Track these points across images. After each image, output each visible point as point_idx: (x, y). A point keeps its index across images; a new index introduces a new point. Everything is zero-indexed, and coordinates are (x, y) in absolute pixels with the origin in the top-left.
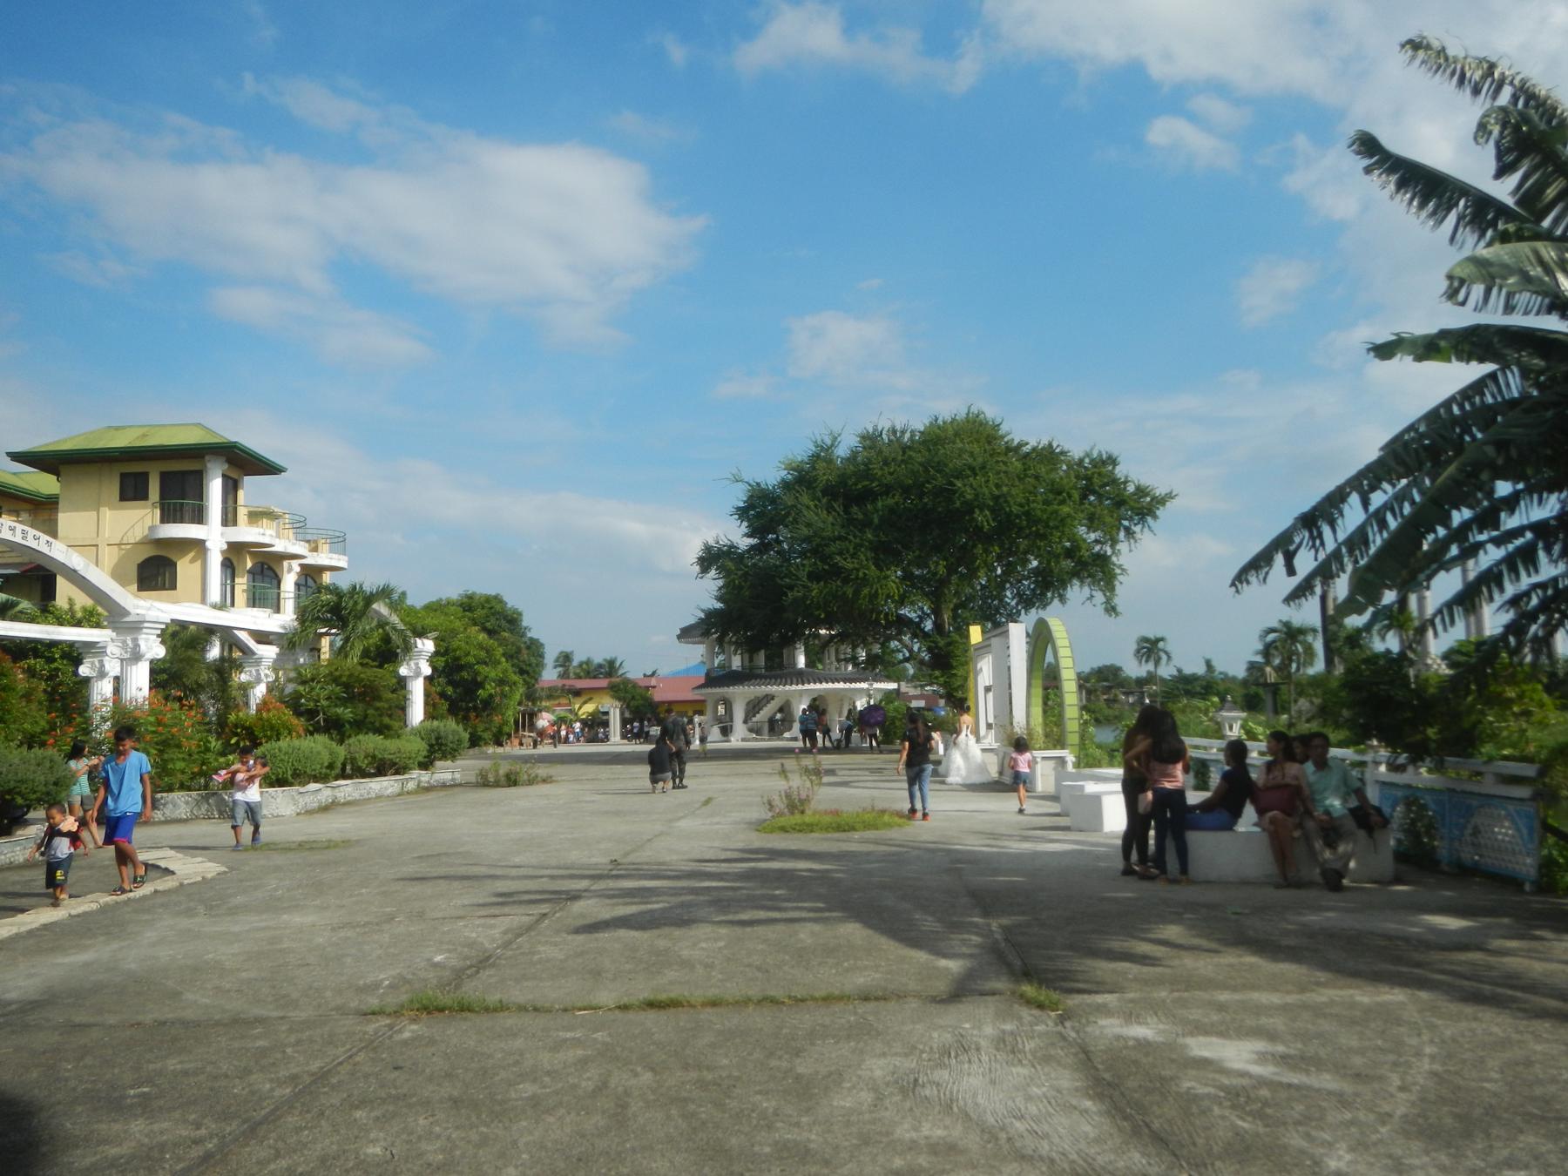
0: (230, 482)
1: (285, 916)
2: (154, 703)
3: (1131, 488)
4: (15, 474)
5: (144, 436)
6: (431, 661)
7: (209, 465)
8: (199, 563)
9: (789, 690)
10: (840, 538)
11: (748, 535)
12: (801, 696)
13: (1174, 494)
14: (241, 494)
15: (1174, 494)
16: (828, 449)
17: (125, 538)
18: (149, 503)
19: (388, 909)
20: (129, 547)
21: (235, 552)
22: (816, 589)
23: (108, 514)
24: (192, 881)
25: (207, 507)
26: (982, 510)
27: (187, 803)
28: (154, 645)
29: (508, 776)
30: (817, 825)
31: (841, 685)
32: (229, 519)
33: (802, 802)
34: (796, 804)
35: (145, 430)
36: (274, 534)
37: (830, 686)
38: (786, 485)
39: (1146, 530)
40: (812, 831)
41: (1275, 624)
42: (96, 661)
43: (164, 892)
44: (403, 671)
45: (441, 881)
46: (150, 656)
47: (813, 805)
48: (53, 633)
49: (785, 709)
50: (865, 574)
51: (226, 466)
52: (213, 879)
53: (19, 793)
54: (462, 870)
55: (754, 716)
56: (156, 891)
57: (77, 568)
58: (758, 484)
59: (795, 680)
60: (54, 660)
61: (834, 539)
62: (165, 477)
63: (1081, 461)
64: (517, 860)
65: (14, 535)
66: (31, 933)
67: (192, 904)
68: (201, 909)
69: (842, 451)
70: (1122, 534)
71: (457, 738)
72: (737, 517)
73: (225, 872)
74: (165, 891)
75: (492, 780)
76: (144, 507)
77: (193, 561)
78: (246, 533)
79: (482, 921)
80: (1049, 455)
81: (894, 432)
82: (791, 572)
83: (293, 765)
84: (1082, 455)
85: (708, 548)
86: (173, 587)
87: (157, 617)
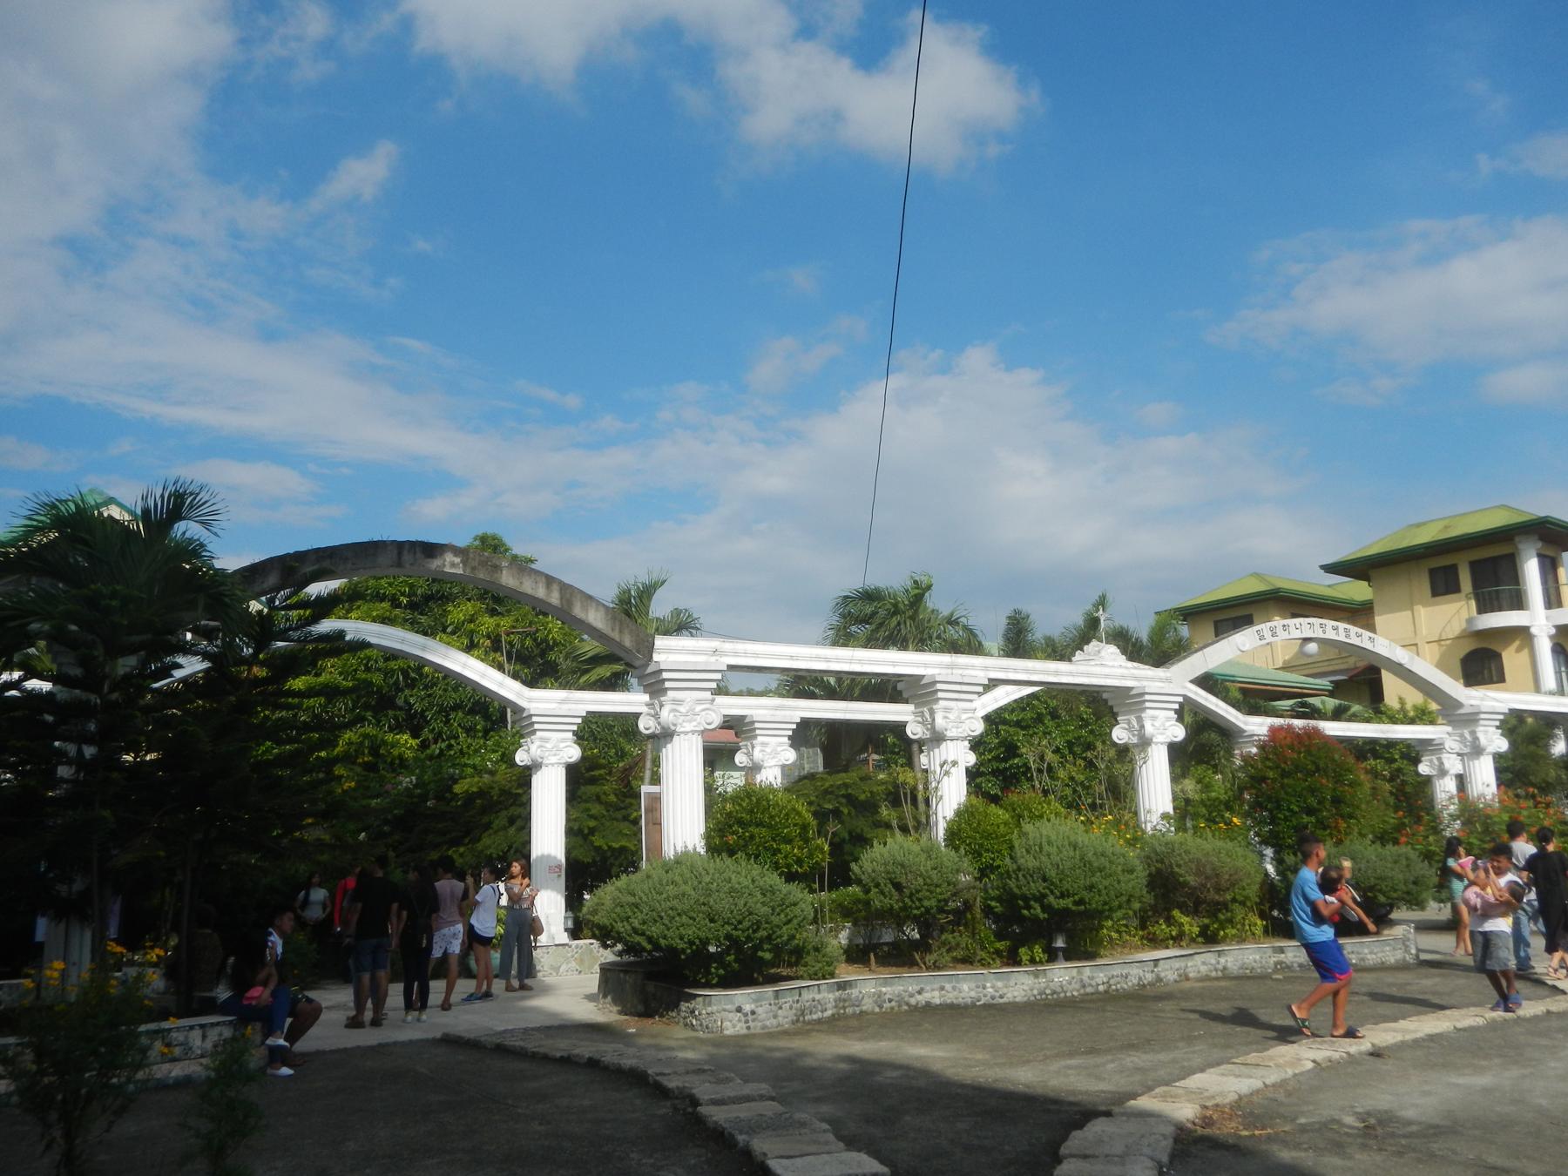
0: (1548, 562)
2: (1504, 801)
4: (1329, 586)
5: (1446, 527)
7: (1521, 546)
14: (1562, 572)
17: (1443, 634)
18: (1462, 595)
20: (1448, 642)
23: (1423, 612)
25: (1525, 591)
28: (1495, 737)
35: (1445, 522)
42: (1434, 758)
46: (1492, 749)
48: (1388, 732)
51: (1540, 545)
53: (1380, 891)
56: (1549, 1012)
57: (1403, 662)
60: (1393, 761)
62: (1475, 567)
65: (1337, 634)
66: (1417, 1043)
76: (1460, 600)
77: (1518, 650)
86: (1502, 679)
87: (1493, 706)
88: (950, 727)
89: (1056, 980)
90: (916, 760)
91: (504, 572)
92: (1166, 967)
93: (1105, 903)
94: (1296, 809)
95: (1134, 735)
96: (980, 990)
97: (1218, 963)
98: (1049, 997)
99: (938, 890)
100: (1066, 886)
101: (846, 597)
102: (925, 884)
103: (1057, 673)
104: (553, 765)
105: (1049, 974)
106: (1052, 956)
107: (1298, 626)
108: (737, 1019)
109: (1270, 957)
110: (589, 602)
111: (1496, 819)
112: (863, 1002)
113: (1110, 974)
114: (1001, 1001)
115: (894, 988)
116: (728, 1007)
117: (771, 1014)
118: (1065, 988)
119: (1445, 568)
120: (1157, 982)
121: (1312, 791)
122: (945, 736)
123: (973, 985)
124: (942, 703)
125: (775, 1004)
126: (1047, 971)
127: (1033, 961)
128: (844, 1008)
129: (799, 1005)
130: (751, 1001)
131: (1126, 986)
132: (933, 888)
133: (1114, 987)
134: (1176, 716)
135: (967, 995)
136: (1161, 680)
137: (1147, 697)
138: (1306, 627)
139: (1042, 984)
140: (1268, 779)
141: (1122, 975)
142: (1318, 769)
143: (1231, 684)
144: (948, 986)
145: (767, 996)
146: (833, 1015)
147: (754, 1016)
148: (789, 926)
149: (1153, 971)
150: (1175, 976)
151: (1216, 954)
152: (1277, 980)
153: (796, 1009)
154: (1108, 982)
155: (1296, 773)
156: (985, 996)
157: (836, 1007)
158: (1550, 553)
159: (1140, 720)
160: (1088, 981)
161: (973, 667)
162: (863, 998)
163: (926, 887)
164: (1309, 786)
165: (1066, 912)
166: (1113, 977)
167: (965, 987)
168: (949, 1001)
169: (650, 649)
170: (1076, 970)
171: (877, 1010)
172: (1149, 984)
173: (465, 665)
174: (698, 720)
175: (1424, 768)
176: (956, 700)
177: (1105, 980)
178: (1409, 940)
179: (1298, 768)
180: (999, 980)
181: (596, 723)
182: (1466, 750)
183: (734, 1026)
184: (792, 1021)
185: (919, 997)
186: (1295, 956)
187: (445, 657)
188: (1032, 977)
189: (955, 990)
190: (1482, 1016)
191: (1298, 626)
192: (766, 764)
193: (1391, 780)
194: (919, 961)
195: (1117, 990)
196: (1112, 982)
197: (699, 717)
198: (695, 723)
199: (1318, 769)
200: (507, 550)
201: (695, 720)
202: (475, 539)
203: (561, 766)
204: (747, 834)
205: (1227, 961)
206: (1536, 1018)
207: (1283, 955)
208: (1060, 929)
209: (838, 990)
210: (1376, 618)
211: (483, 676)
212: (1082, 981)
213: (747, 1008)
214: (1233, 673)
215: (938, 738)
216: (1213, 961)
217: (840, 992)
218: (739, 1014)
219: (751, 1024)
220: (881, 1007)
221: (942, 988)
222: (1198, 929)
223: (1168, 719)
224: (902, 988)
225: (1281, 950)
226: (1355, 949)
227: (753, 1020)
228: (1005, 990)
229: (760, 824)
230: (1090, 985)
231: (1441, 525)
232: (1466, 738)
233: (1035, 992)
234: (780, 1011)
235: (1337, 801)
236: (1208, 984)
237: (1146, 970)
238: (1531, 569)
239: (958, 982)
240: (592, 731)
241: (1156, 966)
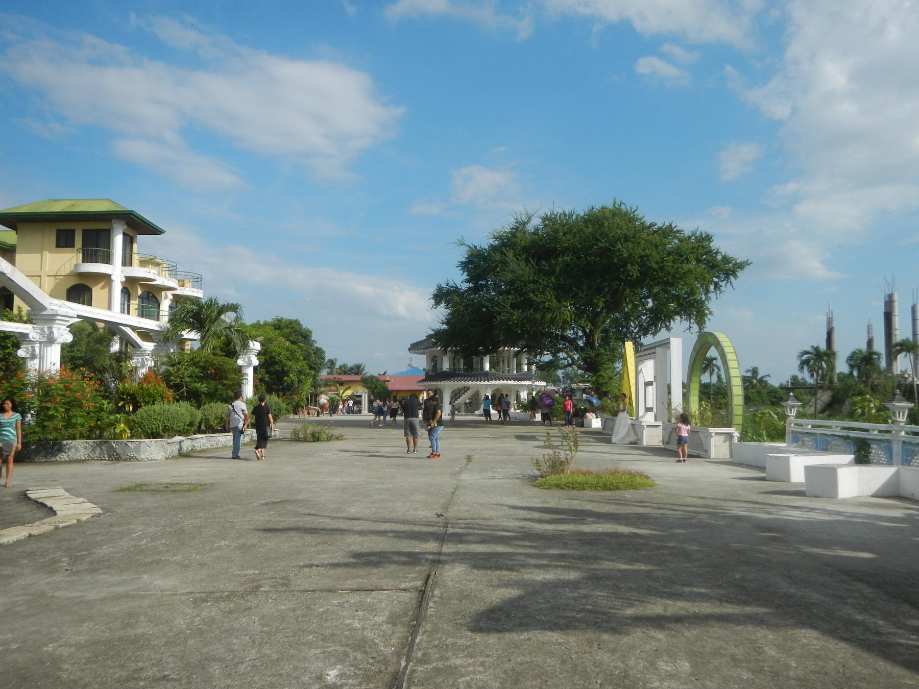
0: (128, 239)
1: (145, 577)
3: (719, 257)
5: (73, 205)
6: (259, 354)
7: (114, 226)
9: (480, 385)
10: (535, 282)
11: (468, 281)
12: (486, 388)
13: (749, 262)
14: (135, 246)
15: (749, 262)
16: (524, 224)
17: (59, 272)
18: (75, 249)
19: (251, 572)
20: (61, 277)
21: (130, 284)
22: (516, 314)
23: (48, 256)
24: (67, 524)
26: (632, 265)
27: (85, 448)
28: (64, 333)
29: (313, 435)
30: (586, 483)
31: (512, 382)
32: (127, 261)
33: (562, 463)
34: (557, 466)
36: (156, 273)
37: (505, 382)
38: (493, 248)
39: (729, 284)
40: (584, 489)
41: (809, 349)
42: (29, 346)
43: (40, 536)
44: (240, 362)
45: (292, 534)
47: (572, 466)
49: (477, 394)
50: (549, 304)
52: (87, 522)
54: (308, 522)
55: (456, 400)
56: (30, 536)
57: (5, 272)
58: (475, 247)
59: (483, 378)
60: (8, 348)
61: (530, 282)
62: (85, 233)
63: (690, 237)
64: (353, 510)
67: (58, 554)
68: (65, 562)
69: (530, 228)
70: (712, 287)
71: (278, 407)
72: (461, 268)
73: (99, 515)
74: (39, 535)
75: (302, 436)
76: (72, 252)
77: (102, 288)
78: (137, 271)
79: (355, 598)
80: (667, 232)
81: (565, 215)
82: (499, 303)
83: (163, 423)
84: (690, 234)
85: (440, 289)
87: (67, 312)
111: (53, 387)
119: (67, 231)
158: (130, 233)
206: (18, 543)
210: (17, 255)
231: (68, 203)
232: (45, 332)
238: (118, 241)
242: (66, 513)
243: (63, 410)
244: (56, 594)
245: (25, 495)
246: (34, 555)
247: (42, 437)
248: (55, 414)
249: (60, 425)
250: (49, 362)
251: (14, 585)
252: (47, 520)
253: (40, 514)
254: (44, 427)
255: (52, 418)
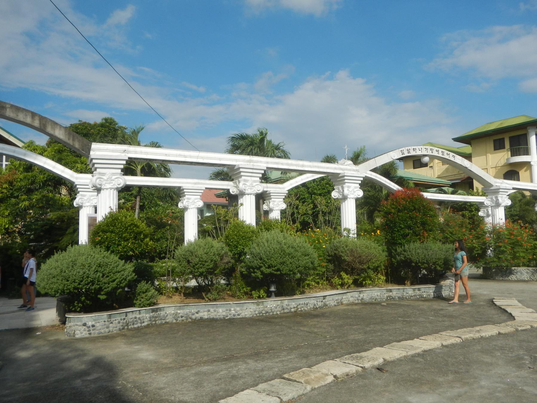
4: (458, 148)
5: (501, 124)
7: (529, 131)
8: (528, 171)
18: (506, 150)
20: (499, 168)
23: (490, 156)
25: (530, 148)
27: (527, 273)
28: (505, 199)
35: (501, 122)
43: (506, 335)
46: (504, 204)
48: (466, 199)
53: (438, 264)
56: (499, 333)
57: (467, 166)
60: (473, 211)
62: (511, 139)
65: (438, 153)
67: (521, 352)
74: (505, 334)
76: (504, 152)
77: (526, 171)
88: (247, 188)
89: (269, 306)
90: (261, 206)
91: (8, 110)
92: (330, 299)
93: (290, 271)
94: (402, 226)
95: (340, 195)
96: (228, 311)
97: (359, 297)
98: (264, 315)
99: (207, 264)
100: (270, 262)
101: (233, 137)
102: (200, 261)
103: (303, 166)
104: (87, 206)
105: (265, 304)
106: (269, 295)
107: (420, 149)
108: (83, 329)
109: (385, 294)
110: (56, 126)
112: (167, 318)
113: (298, 303)
114: (239, 317)
115: (184, 311)
116: (78, 323)
117: (105, 326)
118: (273, 310)
119: (500, 139)
120: (324, 306)
121: (411, 218)
122: (245, 192)
123: (224, 309)
124: (243, 178)
125: (108, 321)
126: (264, 302)
127: (259, 297)
128: (155, 321)
129: (125, 321)
130: (93, 320)
131: (306, 309)
132: (203, 263)
133: (300, 309)
134: (360, 186)
135: (222, 314)
136: (354, 170)
137: (346, 178)
138: (424, 150)
139: (261, 309)
140: (392, 213)
141: (305, 304)
142: (415, 209)
143: (411, 181)
144: (212, 310)
145: (103, 317)
146: (148, 325)
147: (94, 328)
148: (113, 283)
149: (322, 301)
150: (335, 303)
151: (359, 292)
152: (384, 306)
153: (123, 323)
154: (297, 307)
155: (405, 210)
156: (230, 314)
157: (150, 320)
159: (343, 188)
160: (286, 307)
161: (261, 162)
162: (167, 316)
163: (200, 262)
164: (410, 216)
165: (271, 274)
166: (300, 304)
167: (220, 310)
168: (212, 317)
169: (89, 149)
170: (280, 301)
171: (174, 321)
172: (320, 307)
173: (45, 163)
174: (114, 183)
175: (481, 214)
176: (251, 176)
177: (295, 306)
178: (452, 286)
179: (405, 209)
180: (237, 307)
181: (147, 193)
182: (493, 205)
183: (81, 333)
184: (120, 328)
185: (197, 315)
186: (397, 294)
187: (35, 159)
188: (255, 305)
189: (215, 312)
190: (460, 337)
191: (420, 149)
192: (189, 207)
193: (469, 218)
194: (205, 297)
195: (301, 311)
196: (299, 307)
197: (114, 181)
198: (112, 184)
199: (415, 209)
200: (117, 124)
201: (112, 183)
202: (102, 120)
203: (92, 207)
204: (105, 236)
205: (364, 295)
206: (491, 338)
207: (391, 293)
208: (273, 282)
209: (152, 312)
211: (54, 167)
212: (283, 306)
213: (90, 324)
214: (411, 177)
215: (242, 194)
216: (357, 296)
217: (154, 313)
218: (84, 327)
219: (92, 331)
220: (177, 320)
221: (209, 311)
222: (352, 281)
223: (356, 187)
224: (188, 311)
225: (391, 291)
226: (426, 291)
227: (93, 330)
228: (241, 312)
229: (112, 232)
230: (287, 309)
232: (493, 200)
233: (257, 312)
234: (111, 325)
235: (423, 224)
236: (350, 307)
237: (318, 301)
239: (217, 308)
240: (144, 196)
241: (324, 299)
242: (521, 319)
243: (510, 248)
244: (525, 388)
245: (493, 302)
246: (504, 350)
247: (499, 264)
248: (505, 250)
249: (509, 257)
250: (498, 219)
251: (493, 372)
252: (509, 323)
253: (504, 317)
254: (499, 258)
255: (503, 252)
